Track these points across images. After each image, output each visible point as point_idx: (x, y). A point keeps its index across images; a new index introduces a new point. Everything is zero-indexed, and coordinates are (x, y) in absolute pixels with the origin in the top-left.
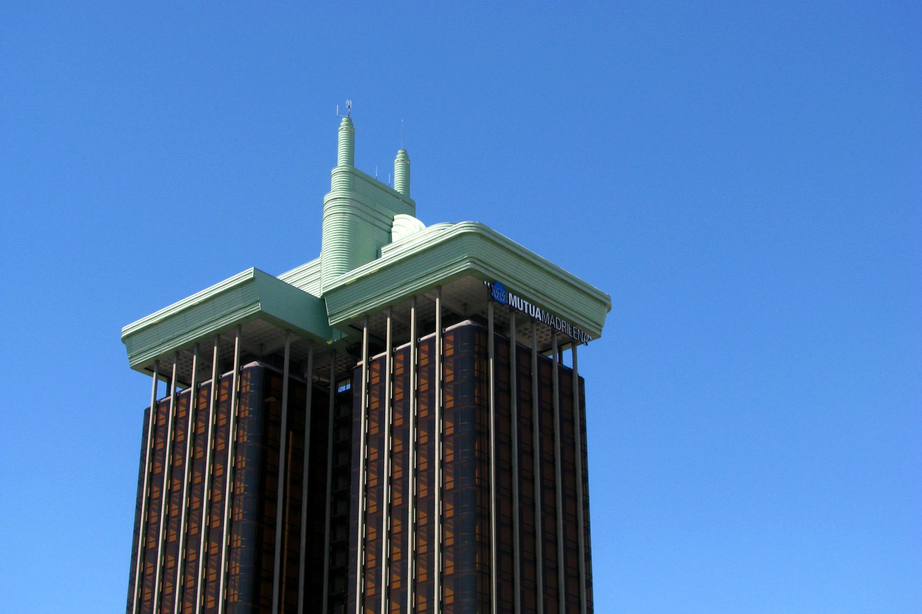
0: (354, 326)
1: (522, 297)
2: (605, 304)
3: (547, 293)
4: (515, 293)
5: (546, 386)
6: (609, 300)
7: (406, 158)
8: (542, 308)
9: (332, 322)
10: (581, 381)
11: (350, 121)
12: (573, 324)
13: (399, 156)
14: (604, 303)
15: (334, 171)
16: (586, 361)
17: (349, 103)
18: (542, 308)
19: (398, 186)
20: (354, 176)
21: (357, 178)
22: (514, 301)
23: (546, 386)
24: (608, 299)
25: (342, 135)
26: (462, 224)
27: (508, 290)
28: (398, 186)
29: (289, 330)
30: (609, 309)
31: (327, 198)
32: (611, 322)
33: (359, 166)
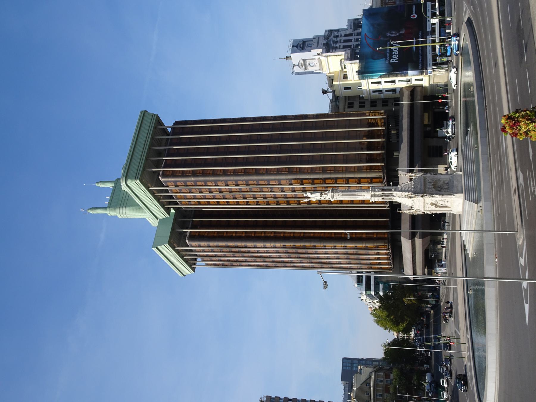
0: (168, 211)
2: (144, 114)
3: (143, 143)
6: (142, 111)
9: (168, 216)
10: (177, 123)
13: (98, 185)
14: (144, 113)
15: (109, 215)
16: (168, 122)
19: (111, 186)
21: (110, 206)
25: (95, 212)
26: (122, 184)
28: (111, 186)
29: (173, 229)
31: (119, 217)
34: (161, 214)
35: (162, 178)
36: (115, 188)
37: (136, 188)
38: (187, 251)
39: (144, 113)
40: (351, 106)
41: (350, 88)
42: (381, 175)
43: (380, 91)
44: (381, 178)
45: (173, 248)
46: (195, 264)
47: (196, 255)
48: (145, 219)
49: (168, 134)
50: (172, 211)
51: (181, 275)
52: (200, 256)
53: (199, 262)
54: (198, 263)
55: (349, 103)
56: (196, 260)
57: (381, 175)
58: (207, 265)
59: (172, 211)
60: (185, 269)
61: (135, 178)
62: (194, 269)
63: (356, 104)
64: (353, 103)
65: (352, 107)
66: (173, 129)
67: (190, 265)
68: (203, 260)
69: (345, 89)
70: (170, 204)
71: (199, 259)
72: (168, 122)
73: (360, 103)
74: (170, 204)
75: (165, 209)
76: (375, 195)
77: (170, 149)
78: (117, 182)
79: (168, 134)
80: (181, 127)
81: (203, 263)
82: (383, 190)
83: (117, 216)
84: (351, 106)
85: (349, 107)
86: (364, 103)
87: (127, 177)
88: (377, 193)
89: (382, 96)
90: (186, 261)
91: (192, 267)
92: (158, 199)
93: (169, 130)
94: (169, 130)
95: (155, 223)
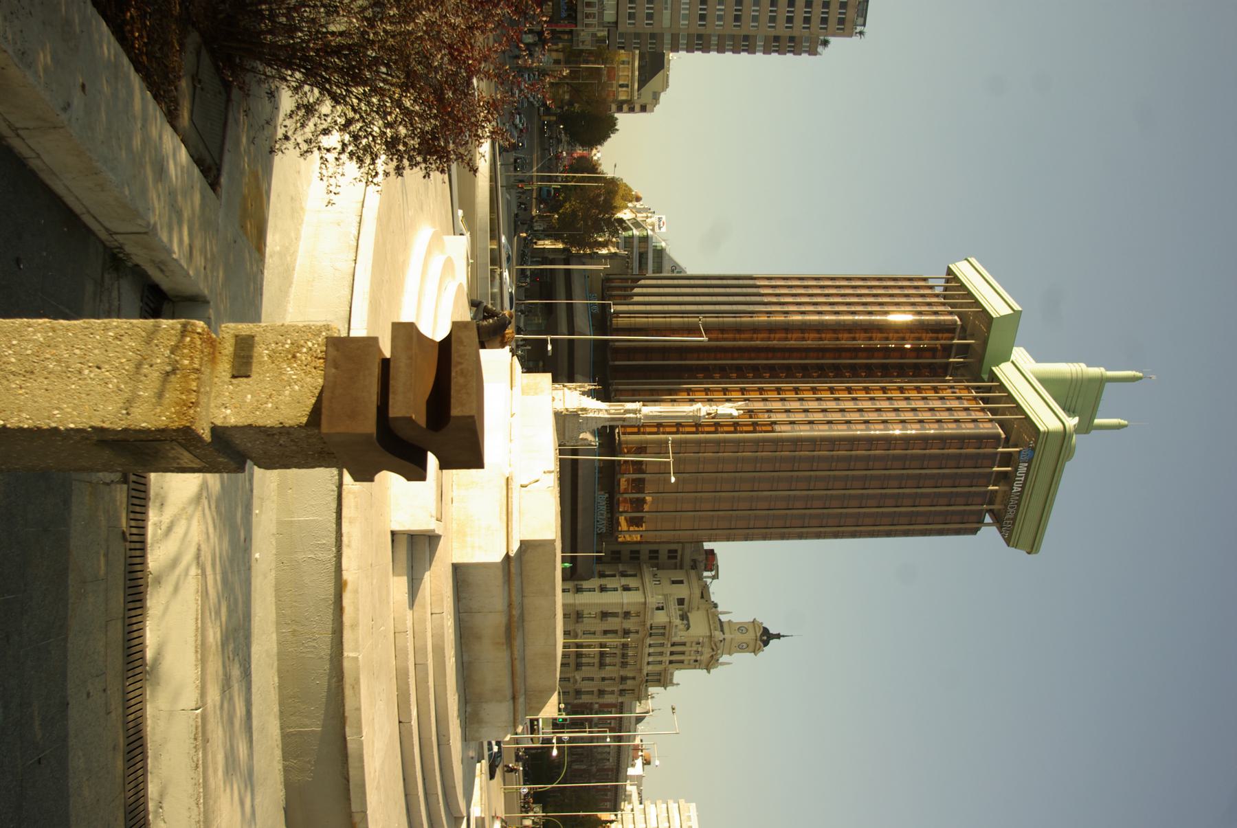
0: (994, 377)
1: (1027, 473)
4: (1028, 468)
5: (968, 498)
7: (1119, 427)
8: (1022, 492)
10: (974, 531)
11: (1140, 378)
12: (1014, 519)
14: (1033, 548)
16: (989, 534)
17: (1154, 377)
18: (1022, 492)
19: (1097, 421)
20: (1102, 381)
22: (1023, 468)
23: (968, 498)
24: (1037, 552)
27: (1030, 462)
28: (1097, 421)
30: (1029, 553)
32: (1019, 554)
33: (1107, 385)
34: (1005, 372)
35: (999, 435)
36: (1092, 418)
37: (1047, 416)
38: (962, 305)
39: (1033, 548)
40: (672, 554)
41: (674, 582)
42: (623, 438)
43: (623, 575)
44: (624, 434)
45: (985, 311)
46: (947, 281)
47: (945, 297)
48: (1037, 361)
49: (988, 511)
50: (985, 377)
51: (973, 260)
52: (937, 296)
53: (939, 285)
54: (942, 282)
55: (676, 557)
56: (946, 289)
57: (623, 438)
58: (925, 279)
59: (985, 377)
60: (964, 270)
61: (1048, 433)
62: (950, 272)
63: (663, 555)
64: (669, 558)
65: (670, 551)
66: (981, 522)
67: (956, 278)
68: (931, 287)
69: (681, 582)
70: (989, 390)
71: (938, 291)
72: (989, 534)
73: (657, 558)
74: (989, 390)
75: (998, 380)
76: (635, 412)
77: (981, 484)
78: (1086, 427)
79: (991, 512)
80: (967, 525)
81: (930, 283)
82: (624, 420)
83: (1088, 366)
84: (672, 554)
85: (676, 551)
86: (651, 558)
87: (1064, 436)
88: (632, 415)
89: (621, 567)
90: (963, 286)
91: (951, 277)
92: (1011, 398)
93: (988, 519)
94: (988, 519)
95: (1019, 354)
